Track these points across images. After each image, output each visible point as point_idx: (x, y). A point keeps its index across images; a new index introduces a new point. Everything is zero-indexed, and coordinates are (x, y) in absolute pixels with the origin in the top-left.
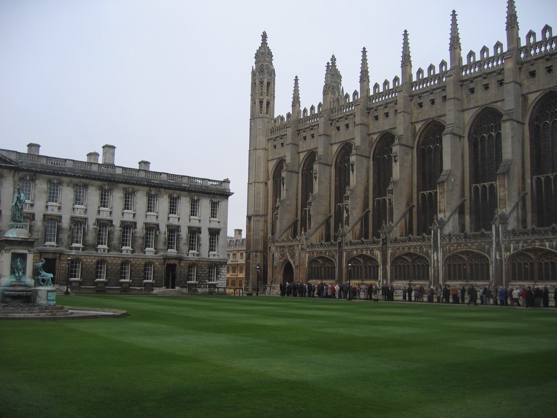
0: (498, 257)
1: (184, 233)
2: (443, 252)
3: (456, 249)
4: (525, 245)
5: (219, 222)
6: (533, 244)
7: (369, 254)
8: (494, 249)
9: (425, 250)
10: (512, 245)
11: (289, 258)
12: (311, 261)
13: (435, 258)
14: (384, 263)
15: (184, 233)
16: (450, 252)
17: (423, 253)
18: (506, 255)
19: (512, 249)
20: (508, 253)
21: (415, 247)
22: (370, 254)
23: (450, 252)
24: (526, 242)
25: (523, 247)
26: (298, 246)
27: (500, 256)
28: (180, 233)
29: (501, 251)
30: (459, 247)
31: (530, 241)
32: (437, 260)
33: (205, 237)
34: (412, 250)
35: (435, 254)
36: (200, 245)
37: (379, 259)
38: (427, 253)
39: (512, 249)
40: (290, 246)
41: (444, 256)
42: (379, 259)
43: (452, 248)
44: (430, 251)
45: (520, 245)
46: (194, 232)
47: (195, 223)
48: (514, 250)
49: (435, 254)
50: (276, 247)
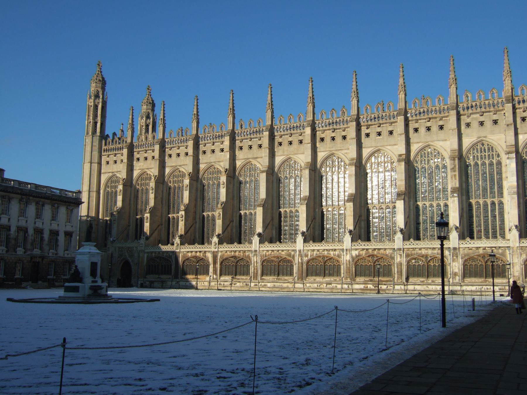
0: (300, 261)
1: (46, 235)
2: (261, 256)
3: (270, 255)
4: (318, 253)
5: (72, 226)
8: (297, 255)
9: (247, 254)
10: (309, 253)
11: (127, 256)
13: (255, 260)
14: (215, 263)
15: (46, 235)
16: (266, 256)
18: (305, 259)
20: (307, 258)
21: (240, 251)
22: (203, 256)
24: (319, 251)
25: (316, 254)
27: (302, 259)
28: (43, 235)
29: (302, 257)
30: (273, 253)
31: (321, 251)
32: (257, 261)
33: (61, 238)
34: (237, 254)
35: (255, 257)
36: (58, 245)
37: (211, 260)
38: (249, 257)
41: (261, 259)
42: (211, 260)
43: (267, 253)
44: (251, 255)
45: (315, 253)
46: (54, 234)
47: (54, 227)
49: (255, 257)
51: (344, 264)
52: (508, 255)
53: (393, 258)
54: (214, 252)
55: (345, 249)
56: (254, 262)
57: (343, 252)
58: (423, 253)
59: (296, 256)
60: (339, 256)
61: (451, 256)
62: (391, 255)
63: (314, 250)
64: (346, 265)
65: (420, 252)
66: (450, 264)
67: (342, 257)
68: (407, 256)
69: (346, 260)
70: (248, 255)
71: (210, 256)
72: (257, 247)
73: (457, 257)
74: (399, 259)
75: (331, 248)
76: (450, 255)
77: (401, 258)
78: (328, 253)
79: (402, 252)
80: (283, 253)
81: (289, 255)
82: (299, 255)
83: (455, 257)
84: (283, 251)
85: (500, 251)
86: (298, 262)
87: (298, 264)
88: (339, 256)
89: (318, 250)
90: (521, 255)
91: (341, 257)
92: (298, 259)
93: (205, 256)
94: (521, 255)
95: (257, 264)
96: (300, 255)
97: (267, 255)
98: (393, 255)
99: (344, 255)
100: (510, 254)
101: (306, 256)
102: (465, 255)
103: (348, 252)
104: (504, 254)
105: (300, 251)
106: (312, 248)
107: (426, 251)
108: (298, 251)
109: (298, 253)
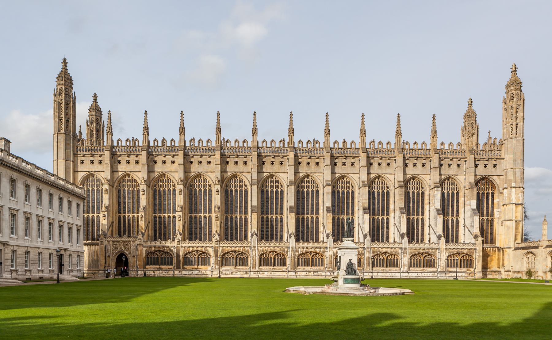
0: (292, 255)
3: (267, 250)
4: (307, 249)
6: (311, 249)
7: (203, 250)
8: (290, 251)
9: (246, 249)
10: (300, 249)
12: (148, 254)
13: (254, 254)
14: (216, 256)
16: (263, 251)
17: (245, 251)
18: (297, 254)
19: (300, 251)
20: (298, 253)
23: (263, 251)
25: (306, 250)
26: (134, 242)
27: (294, 254)
30: (269, 249)
39: (300, 251)
40: (124, 242)
43: (264, 249)
44: (250, 250)
45: (304, 249)
48: (301, 252)
50: (109, 241)
51: (327, 257)
52: (438, 254)
53: (363, 254)
54: (215, 247)
55: (328, 246)
56: (253, 256)
57: (327, 249)
58: (384, 251)
59: (289, 251)
60: (323, 252)
61: (403, 253)
62: (362, 252)
63: (303, 248)
64: (329, 258)
65: (382, 250)
66: (402, 258)
67: (326, 252)
68: (373, 252)
69: (329, 255)
70: (248, 251)
71: (211, 251)
72: (255, 243)
73: (407, 254)
74: (367, 255)
75: (317, 246)
76: (402, 253)
77: (369, 254)
78: (315, 250)
79: (370, 250)
80: (278, 249)
81: (284, 251)
82: (291, 251)
83: (405, 254)
84: (278, 247)
85: (433, 251)
86: (291, 256)
87: (291, 257)
88: (323, 252)
89: (307, 248)
90: (445, 253)
91: (325, 253)
92: (291, 254)
93: (207, 251)
94: (445, 253)
95: (256, 257)
96: (293, 251)
97: (264, 250)
98: (363, 252)
99: (327, 251)
100: (439, 252)
101: (298, 251)
102: (411, 253)
103: (331, 249)
104: (435, 252)
105: (292, 248)
106: (302, 246)
107: (386, 250)
108: (291, 248)
109: (291, 249)
